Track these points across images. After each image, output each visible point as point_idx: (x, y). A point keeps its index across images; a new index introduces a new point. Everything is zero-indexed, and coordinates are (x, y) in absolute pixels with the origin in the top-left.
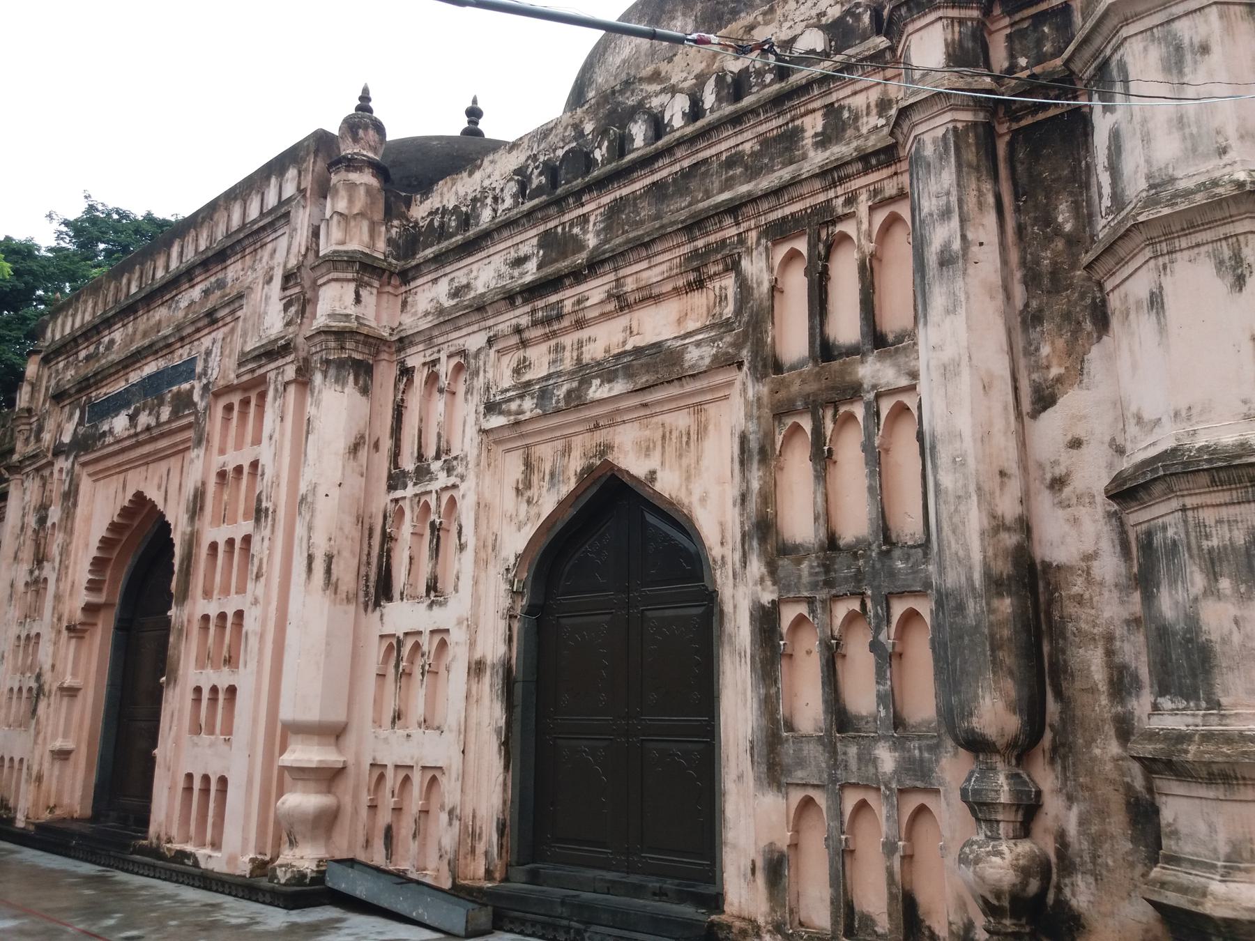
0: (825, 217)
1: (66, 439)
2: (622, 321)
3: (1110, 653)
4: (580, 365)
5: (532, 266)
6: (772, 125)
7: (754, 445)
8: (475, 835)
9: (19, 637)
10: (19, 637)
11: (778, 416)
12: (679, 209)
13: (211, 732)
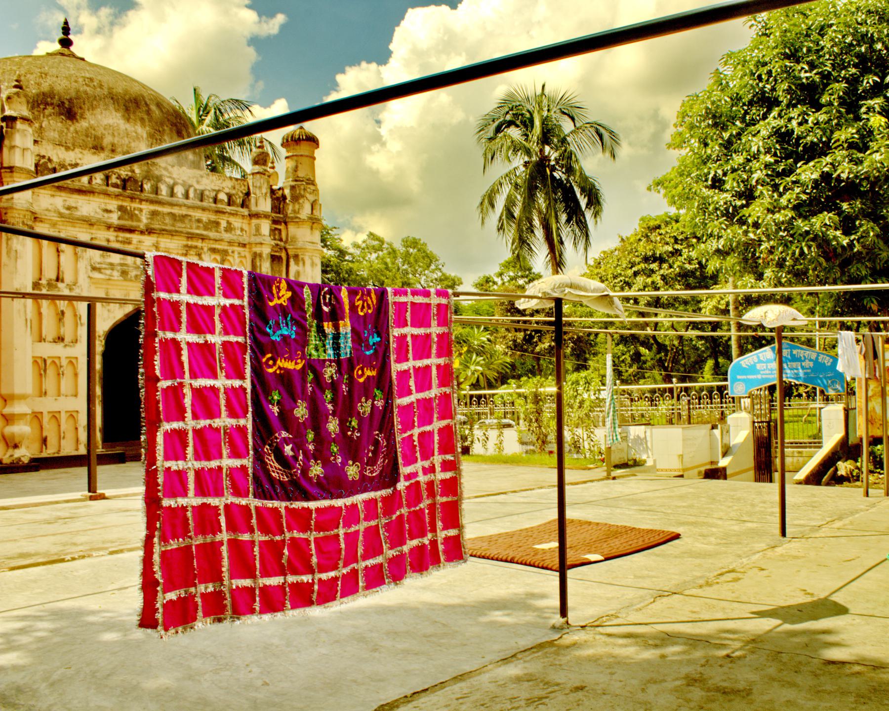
0: (225, 252)
6: (213, 217)
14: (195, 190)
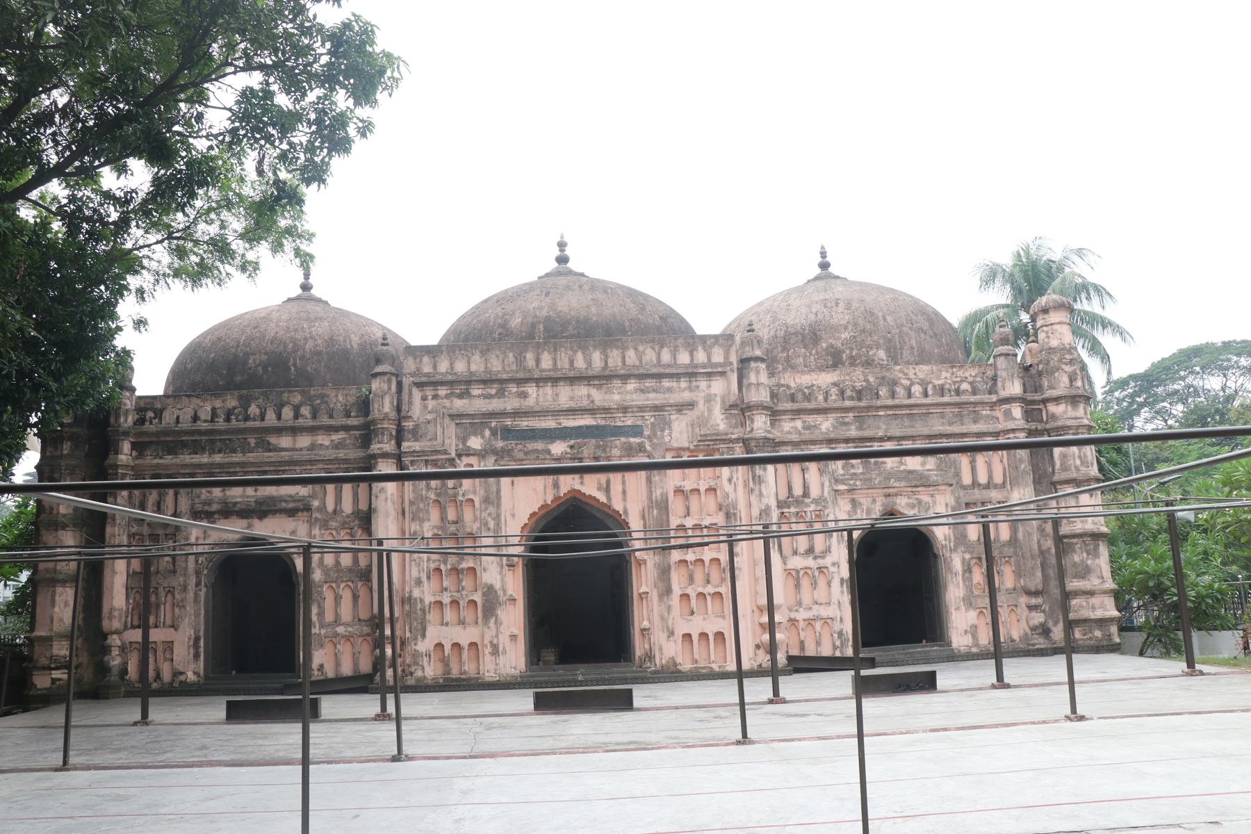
10: (438, 570)
14: (934, 386)
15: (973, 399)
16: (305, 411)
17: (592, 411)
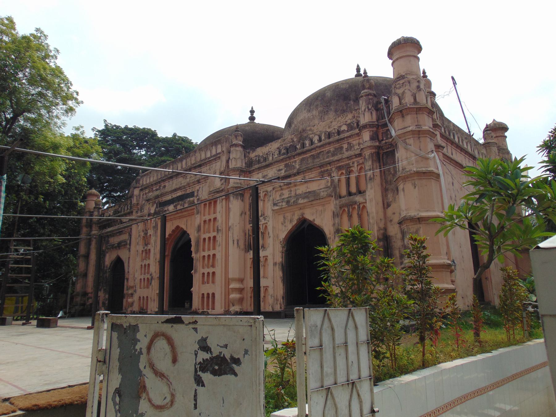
1: (152, 211)
2: (306, 185)
3: (399, 251)
4: (296, 195)
5: (283, 171)
6: (337, 145)
7: (336, 213)
8: (277, 300)
9: (142, 265)
10: (142, 265)
11: (340, 208)
12: (318, 162)
13: (208, 283)
15: (346, 135)
16: (129, 208)
17: (180, 189)
